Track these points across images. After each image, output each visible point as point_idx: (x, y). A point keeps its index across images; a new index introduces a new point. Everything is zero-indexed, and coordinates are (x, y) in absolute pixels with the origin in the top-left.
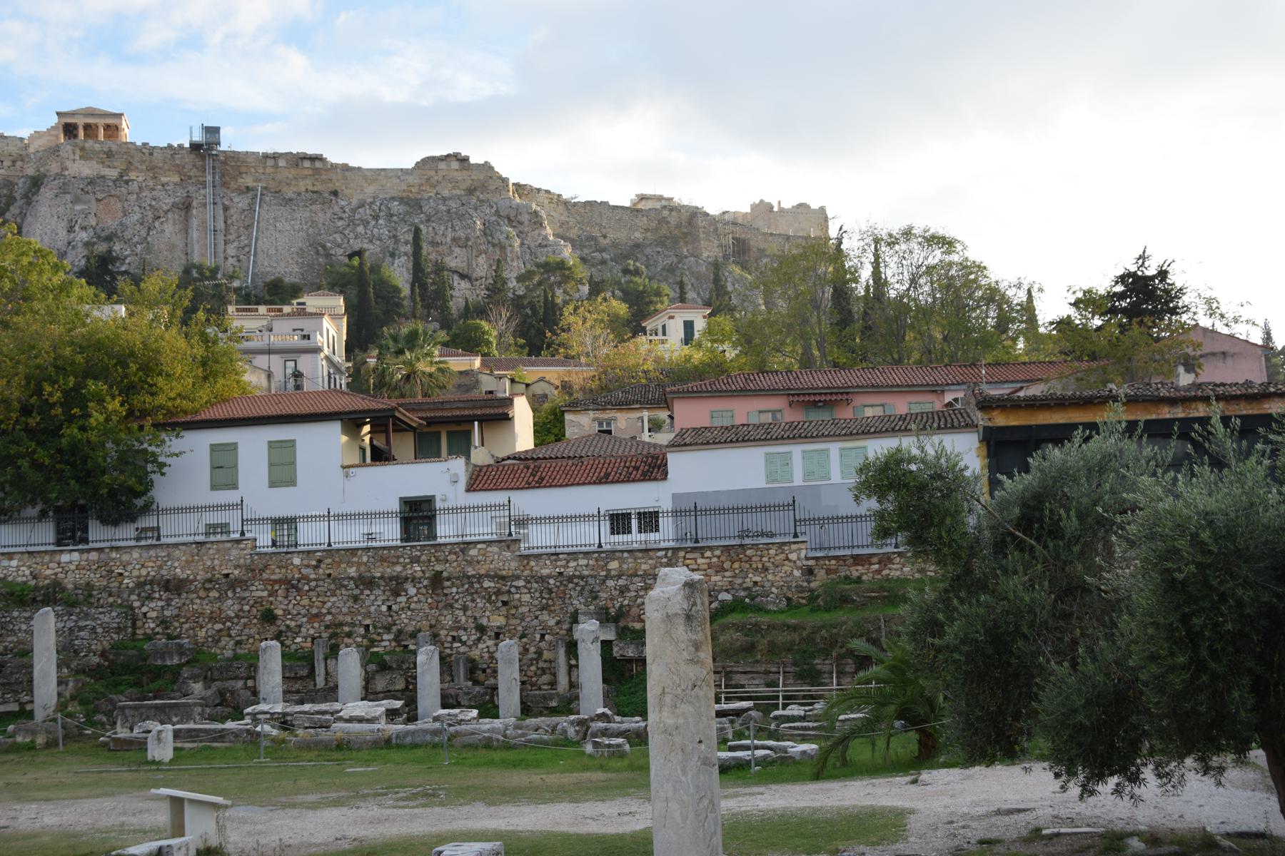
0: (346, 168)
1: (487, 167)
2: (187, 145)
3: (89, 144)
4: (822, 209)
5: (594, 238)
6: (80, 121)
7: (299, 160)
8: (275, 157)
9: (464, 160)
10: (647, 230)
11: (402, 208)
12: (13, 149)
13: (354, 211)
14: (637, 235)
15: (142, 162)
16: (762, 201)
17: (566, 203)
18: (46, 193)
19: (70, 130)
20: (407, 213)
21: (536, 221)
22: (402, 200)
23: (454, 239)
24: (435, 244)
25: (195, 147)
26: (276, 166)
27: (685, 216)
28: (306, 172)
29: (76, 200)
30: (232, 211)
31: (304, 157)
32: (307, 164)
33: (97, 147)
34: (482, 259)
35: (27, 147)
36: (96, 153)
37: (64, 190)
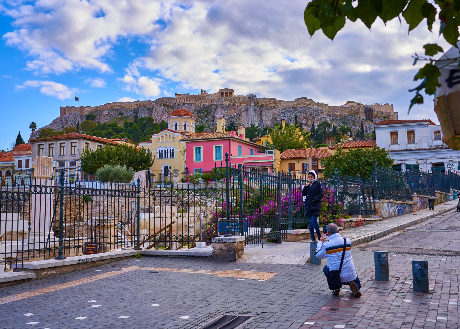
3: (227, 98)
6: (224, 91)
8: (265, 99)
9: (306, 98)
11: (293, 110)
12: (211, 98)
17: (330, 107)
18: (219, 109)
19: (222, 93)
21: (322, 112)
24: (299, 118)
26: (265, 101)
29: (225, 110)
31: (271, 99)
32: (272, 100)
33: (229, 98)
34: (310, 121)
37: (222, 108)
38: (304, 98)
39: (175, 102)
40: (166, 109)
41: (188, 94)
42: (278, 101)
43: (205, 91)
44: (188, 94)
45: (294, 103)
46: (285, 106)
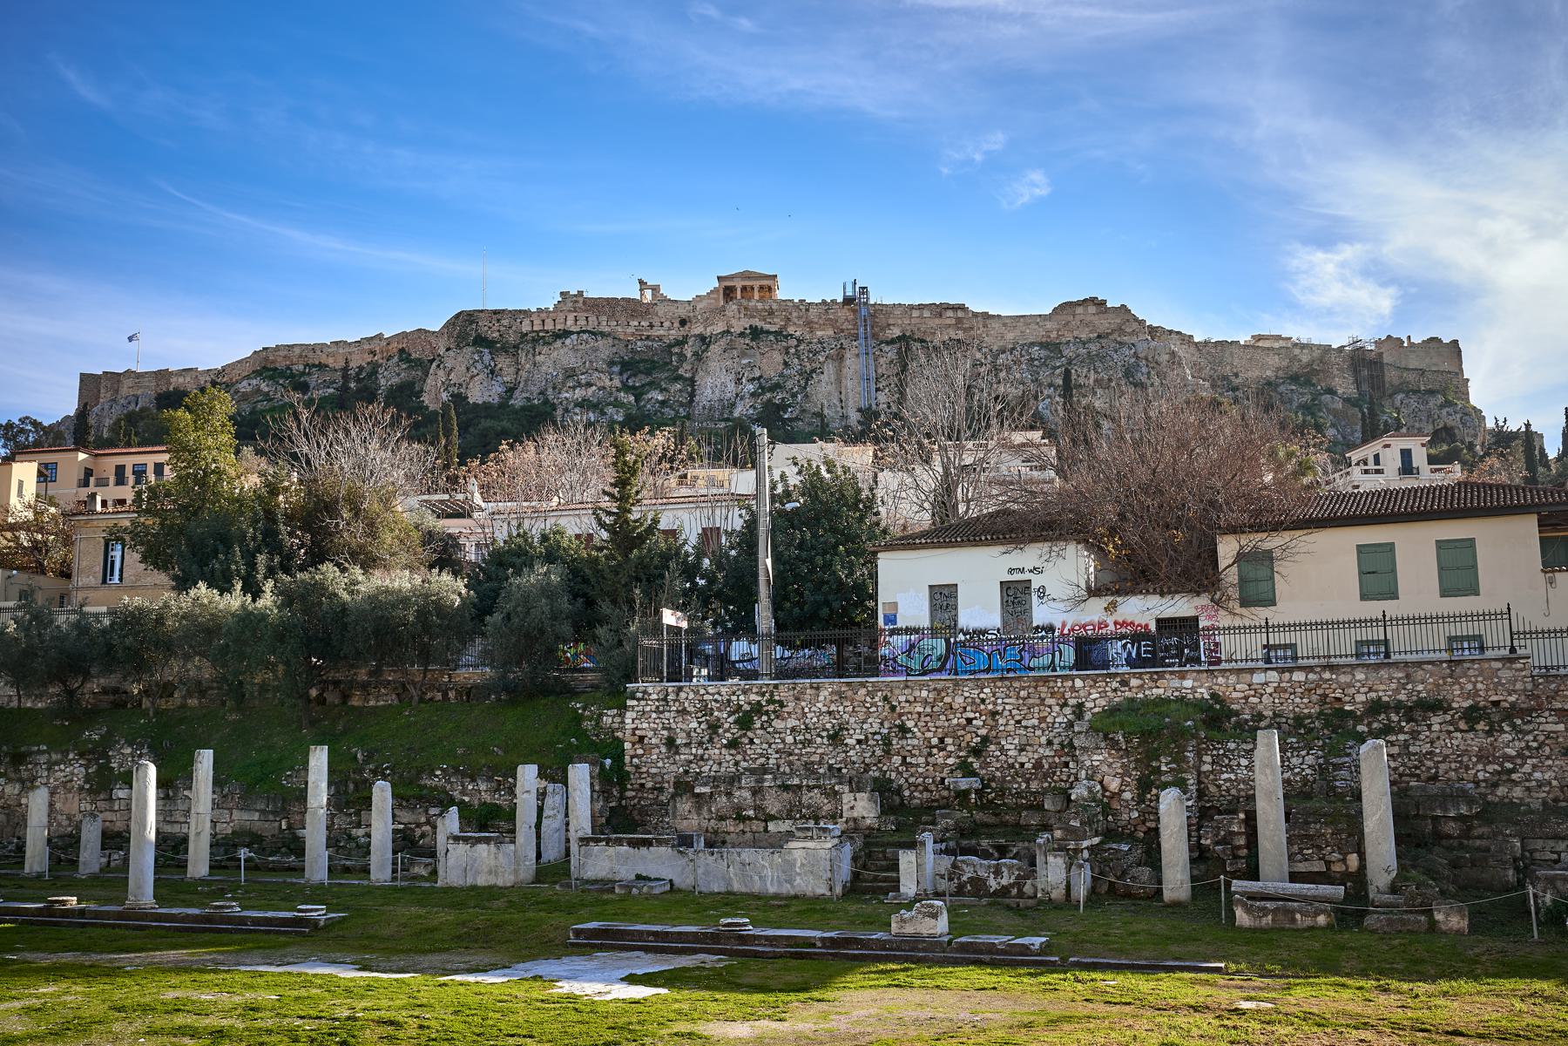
0: (986, 316)
1: (1124, 309)
2: (840, 300)
4: (1455, 342)
5: (1225, 378)
6: (739, 284)
7: (940, 309)
8: (921, 307)
10: (1279, 369)
11: (1043, 353)
12: (682, 312)
13: (996, 357)
14: (1269, 373)
15: (799, 318)
16: (1389, 337)
18: (715, 349)
19: (728, 292)
20: (1047, 357)
22: (1042, 345)
23: (1096, 381)
25: (848, 301)
27: (1317, 353)
28: (948, 321)
29: (743, 355)
30: (882, 360)
32: (950, 313)
35: (694, 308)
36: (757, 310)
38: (1093, 300)
39: (526, 328)
40: (487, 358)
41: (580, 293)
42: (976, 315)
43: (655, 289)
44: (580, 293)
45: (1049, 325)
46: (1010, 336)
